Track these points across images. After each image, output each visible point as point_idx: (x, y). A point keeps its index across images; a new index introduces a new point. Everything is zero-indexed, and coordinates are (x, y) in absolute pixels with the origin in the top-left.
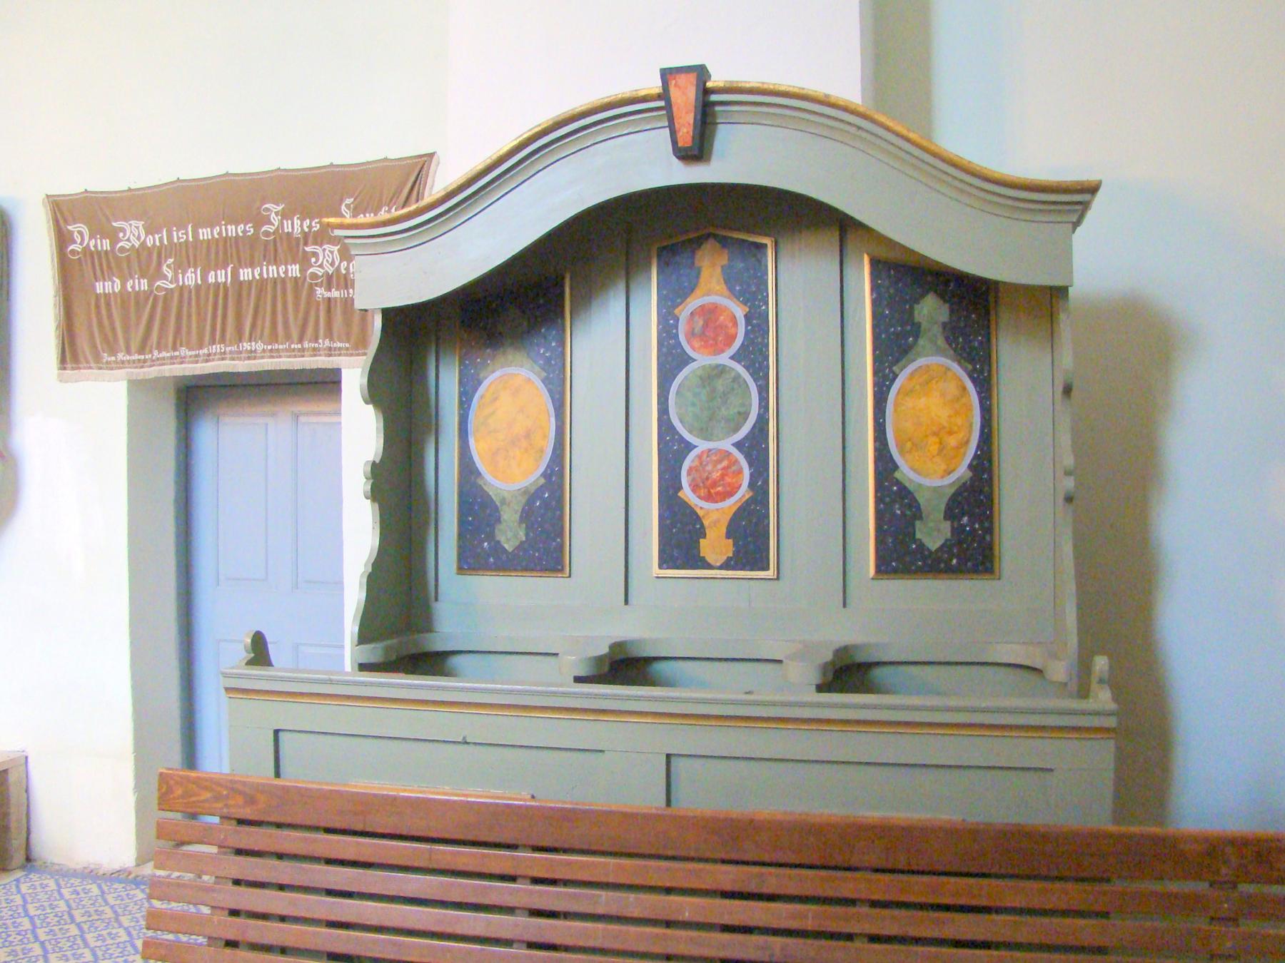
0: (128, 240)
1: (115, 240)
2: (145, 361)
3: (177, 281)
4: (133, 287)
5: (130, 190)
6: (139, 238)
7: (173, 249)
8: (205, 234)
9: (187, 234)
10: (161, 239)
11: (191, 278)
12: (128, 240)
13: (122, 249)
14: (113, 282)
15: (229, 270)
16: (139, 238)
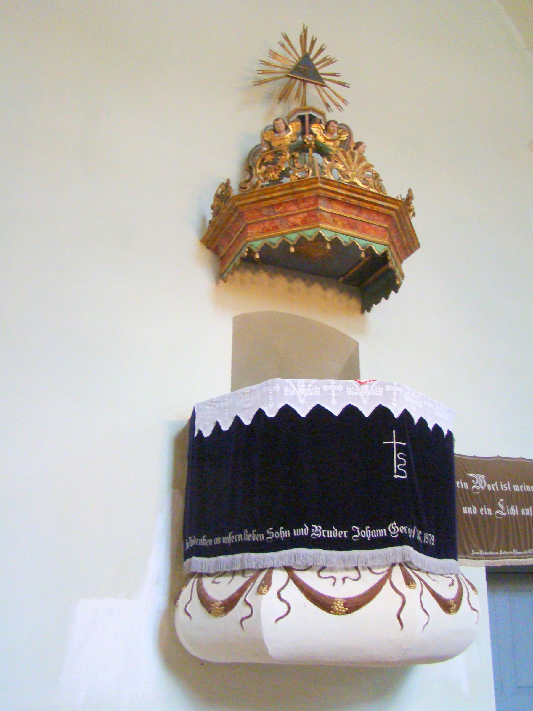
0: (478, 485)
1: (471, 484)
2: (498, 556)
3: (507, 512)
4: (484, 512)
5: (475, 457)
6: (483, 485)
7: (501, 494)
8: (516, 488)
9: (507, 486)
10: (495, 487)
11: (513, 511)
12: (478, 485)
13: (475, 490)
14: (472, 508)
15: (531, 509)
16: (483, 485)
